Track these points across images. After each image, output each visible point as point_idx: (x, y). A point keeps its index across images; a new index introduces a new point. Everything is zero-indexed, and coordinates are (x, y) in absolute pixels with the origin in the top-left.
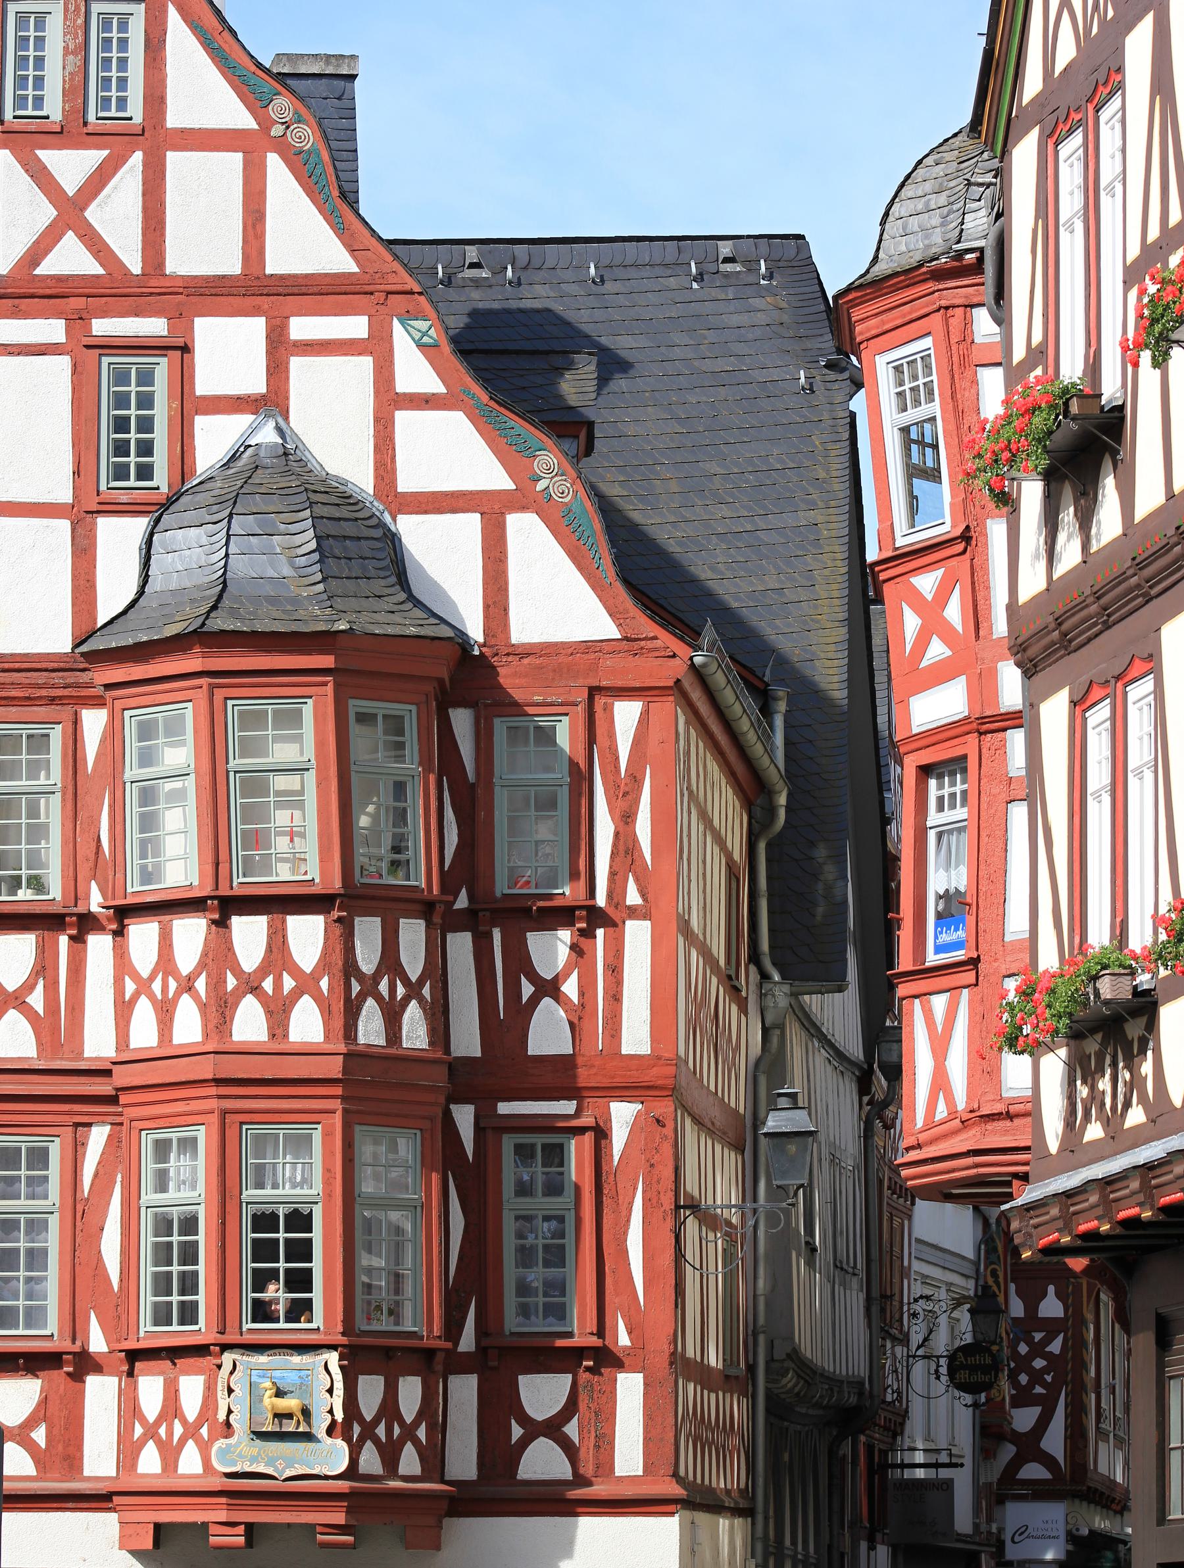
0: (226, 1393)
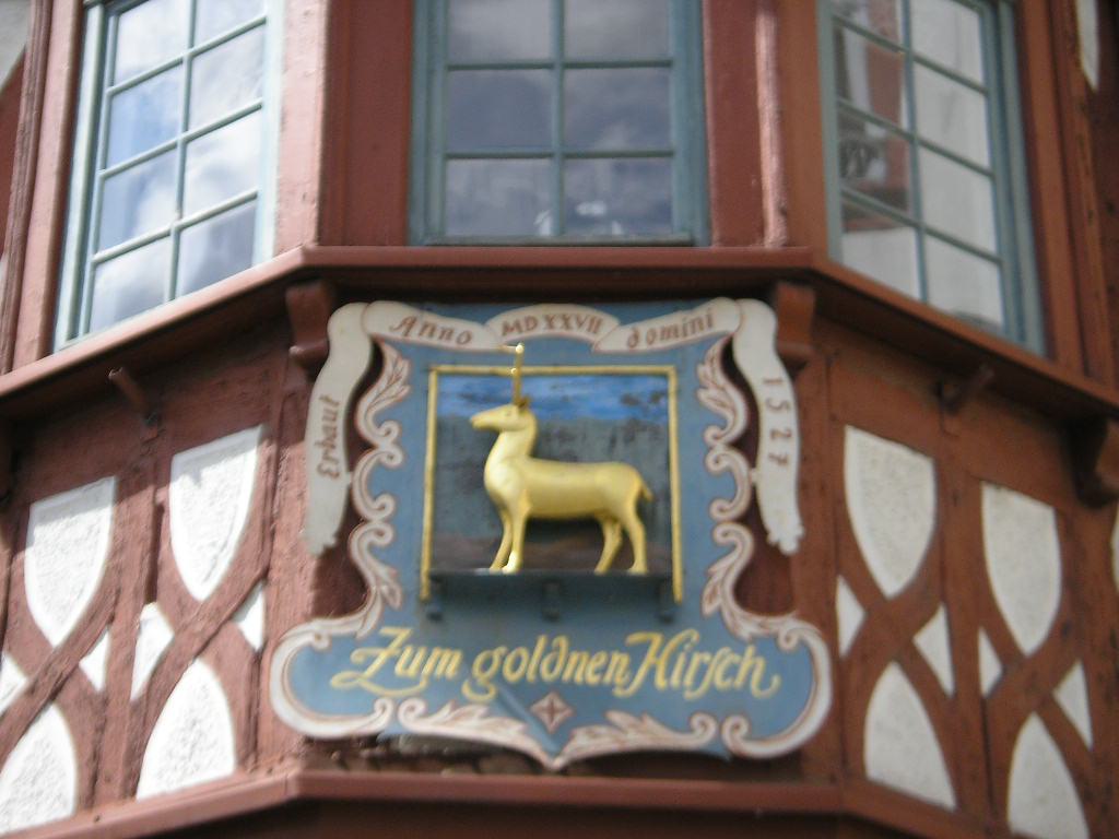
0: (339, 453)
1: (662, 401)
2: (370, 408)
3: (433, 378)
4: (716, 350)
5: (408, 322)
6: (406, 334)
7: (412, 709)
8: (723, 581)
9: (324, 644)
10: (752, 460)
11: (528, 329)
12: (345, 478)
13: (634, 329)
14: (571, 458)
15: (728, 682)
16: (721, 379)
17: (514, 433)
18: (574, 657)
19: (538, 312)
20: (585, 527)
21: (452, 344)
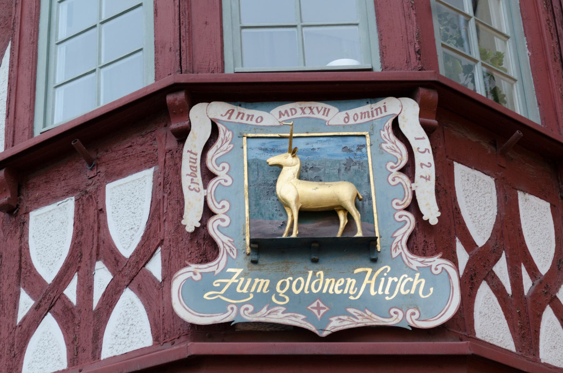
1: (364, 150)
2: (213, 157)
3: (245, 138)
4: (390, 122)
5: (230, 112)
6: (229, 118)
7: (247, 309)
8: (401, 240)
9: (198, 277)
10: (412, 179)
11: (292, 115)
12: (203, 192)
13: (347, 114)
14: (318, 179)
15: (408, 291)
16: (393, 137)
17: (291, 165)
18: (328, 281)
19: (296, 105)
20: (328, 213)
21: (253, 122)
